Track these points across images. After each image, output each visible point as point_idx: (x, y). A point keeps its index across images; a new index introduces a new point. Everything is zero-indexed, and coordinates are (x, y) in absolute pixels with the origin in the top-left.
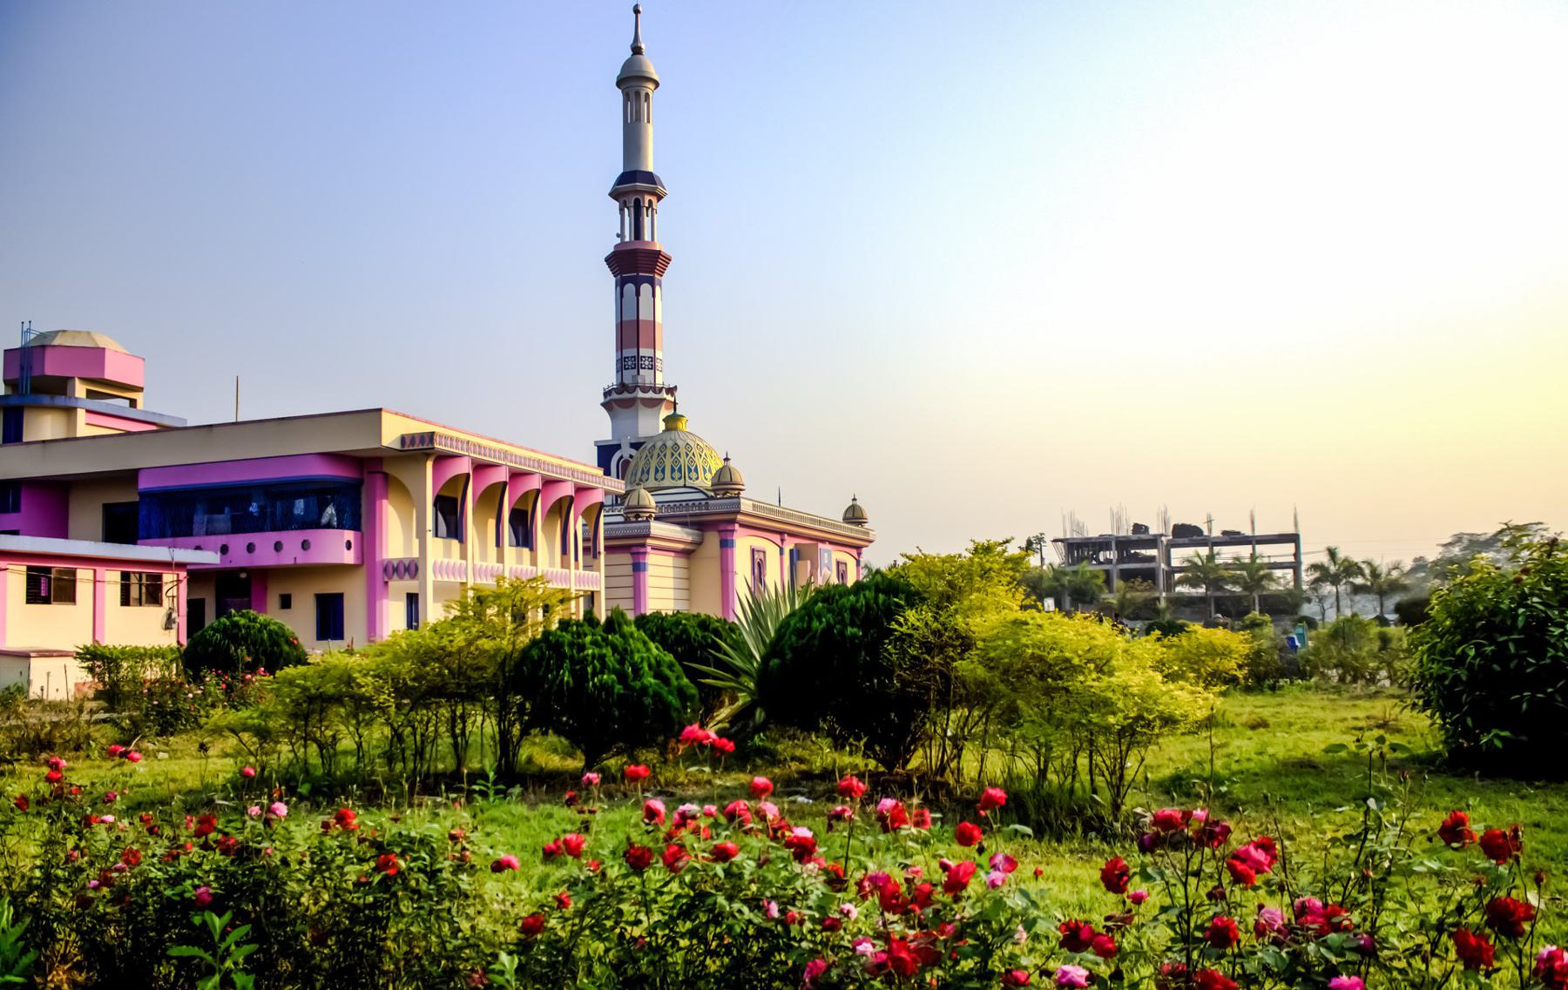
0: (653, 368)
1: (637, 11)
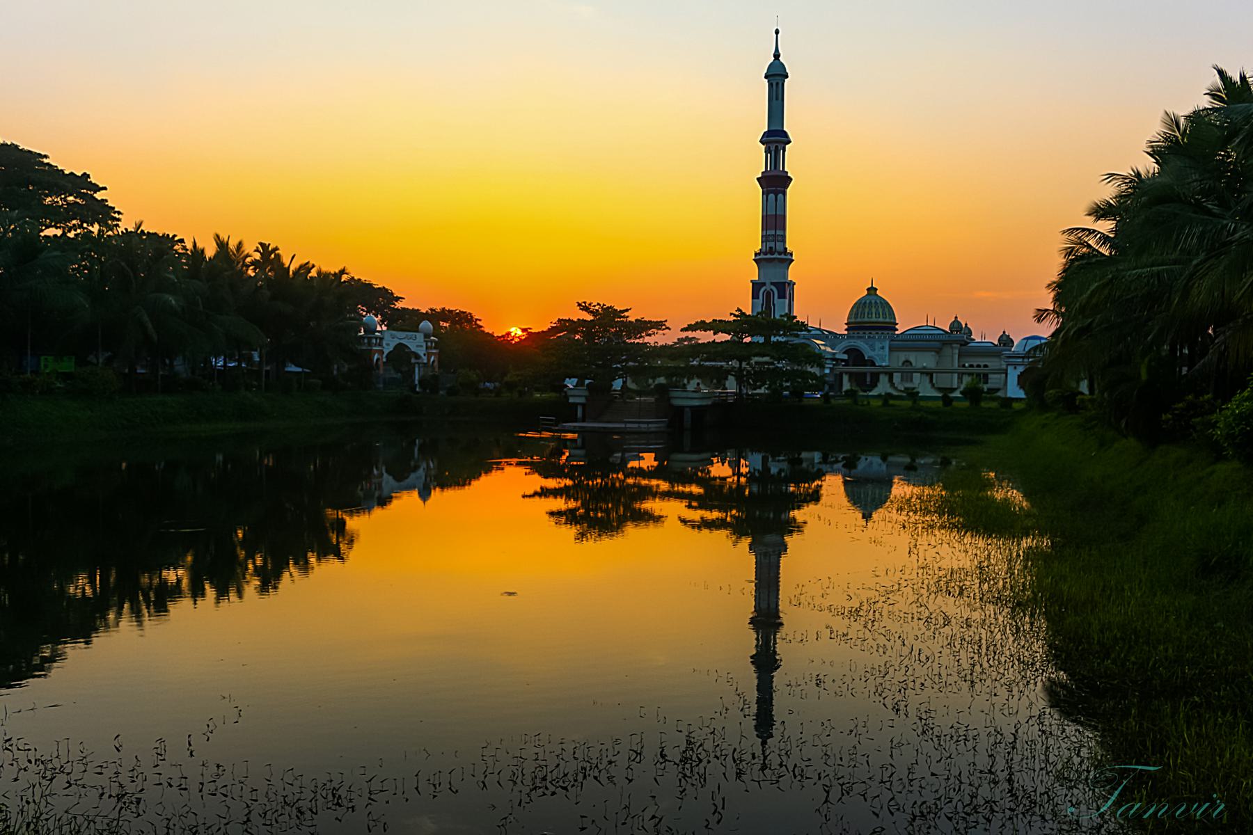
0: (784, 241)
1: (777, 32)
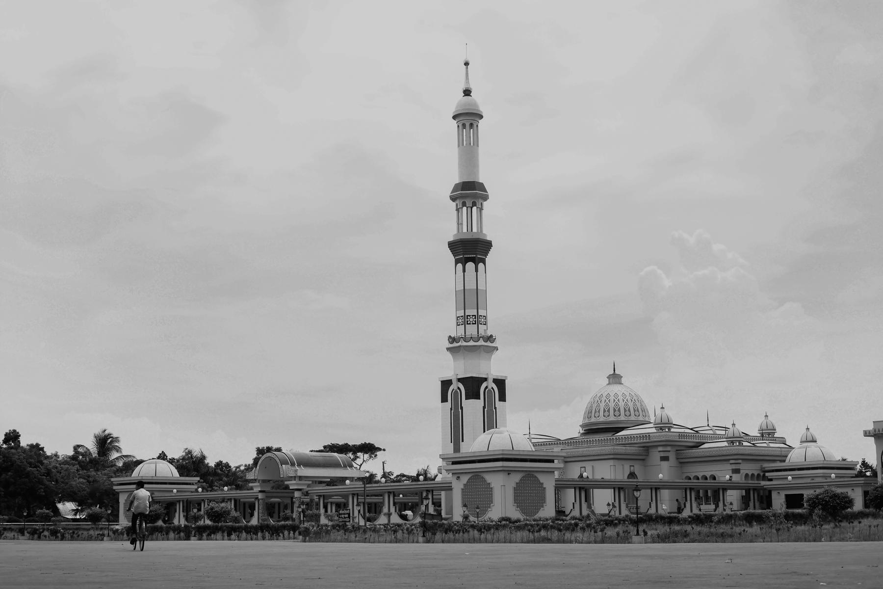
1: (467, 64)
